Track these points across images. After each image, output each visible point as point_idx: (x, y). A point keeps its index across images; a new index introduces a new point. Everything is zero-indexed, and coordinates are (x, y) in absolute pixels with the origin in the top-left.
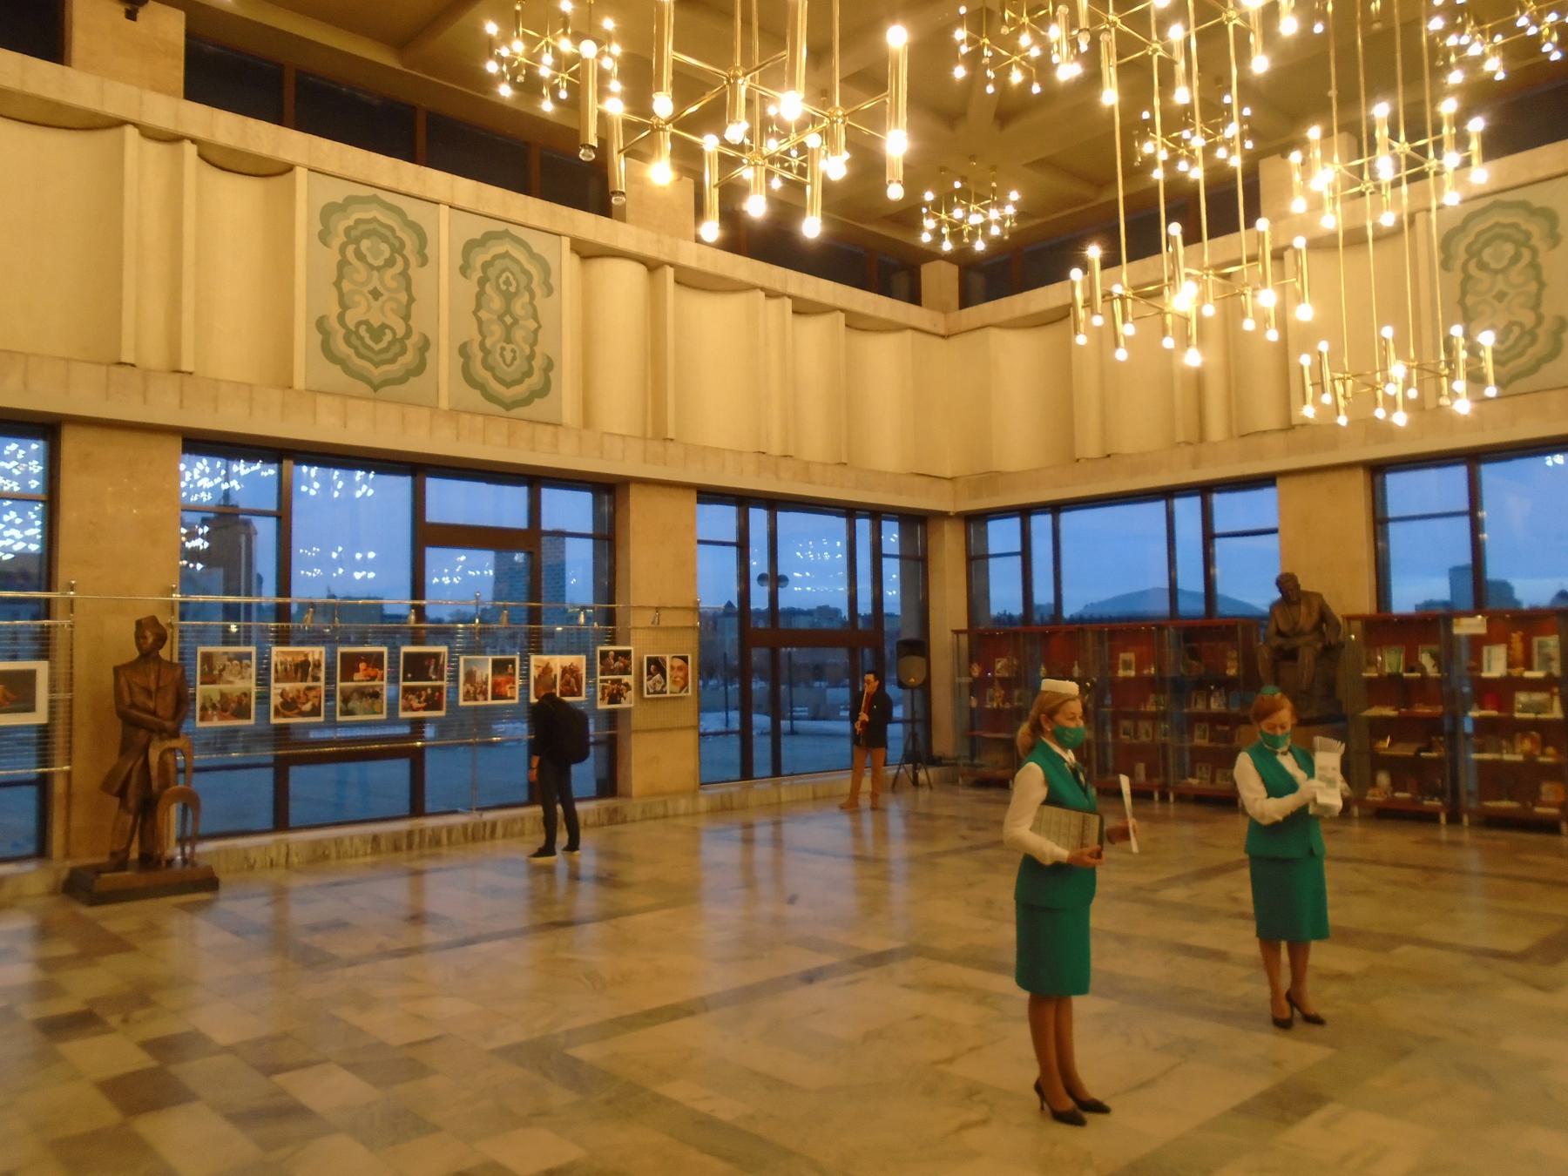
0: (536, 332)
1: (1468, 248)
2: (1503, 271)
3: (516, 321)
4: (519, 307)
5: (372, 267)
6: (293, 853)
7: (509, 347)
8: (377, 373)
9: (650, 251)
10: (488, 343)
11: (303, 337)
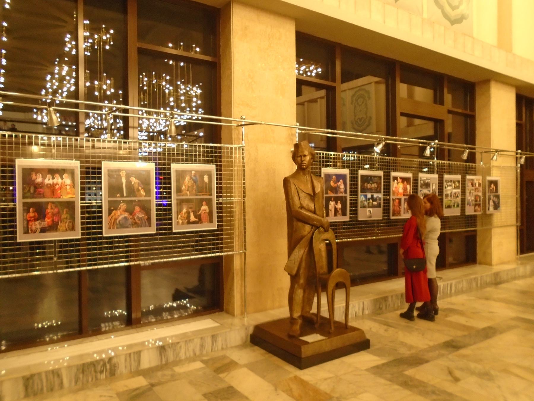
6: (366, 307)
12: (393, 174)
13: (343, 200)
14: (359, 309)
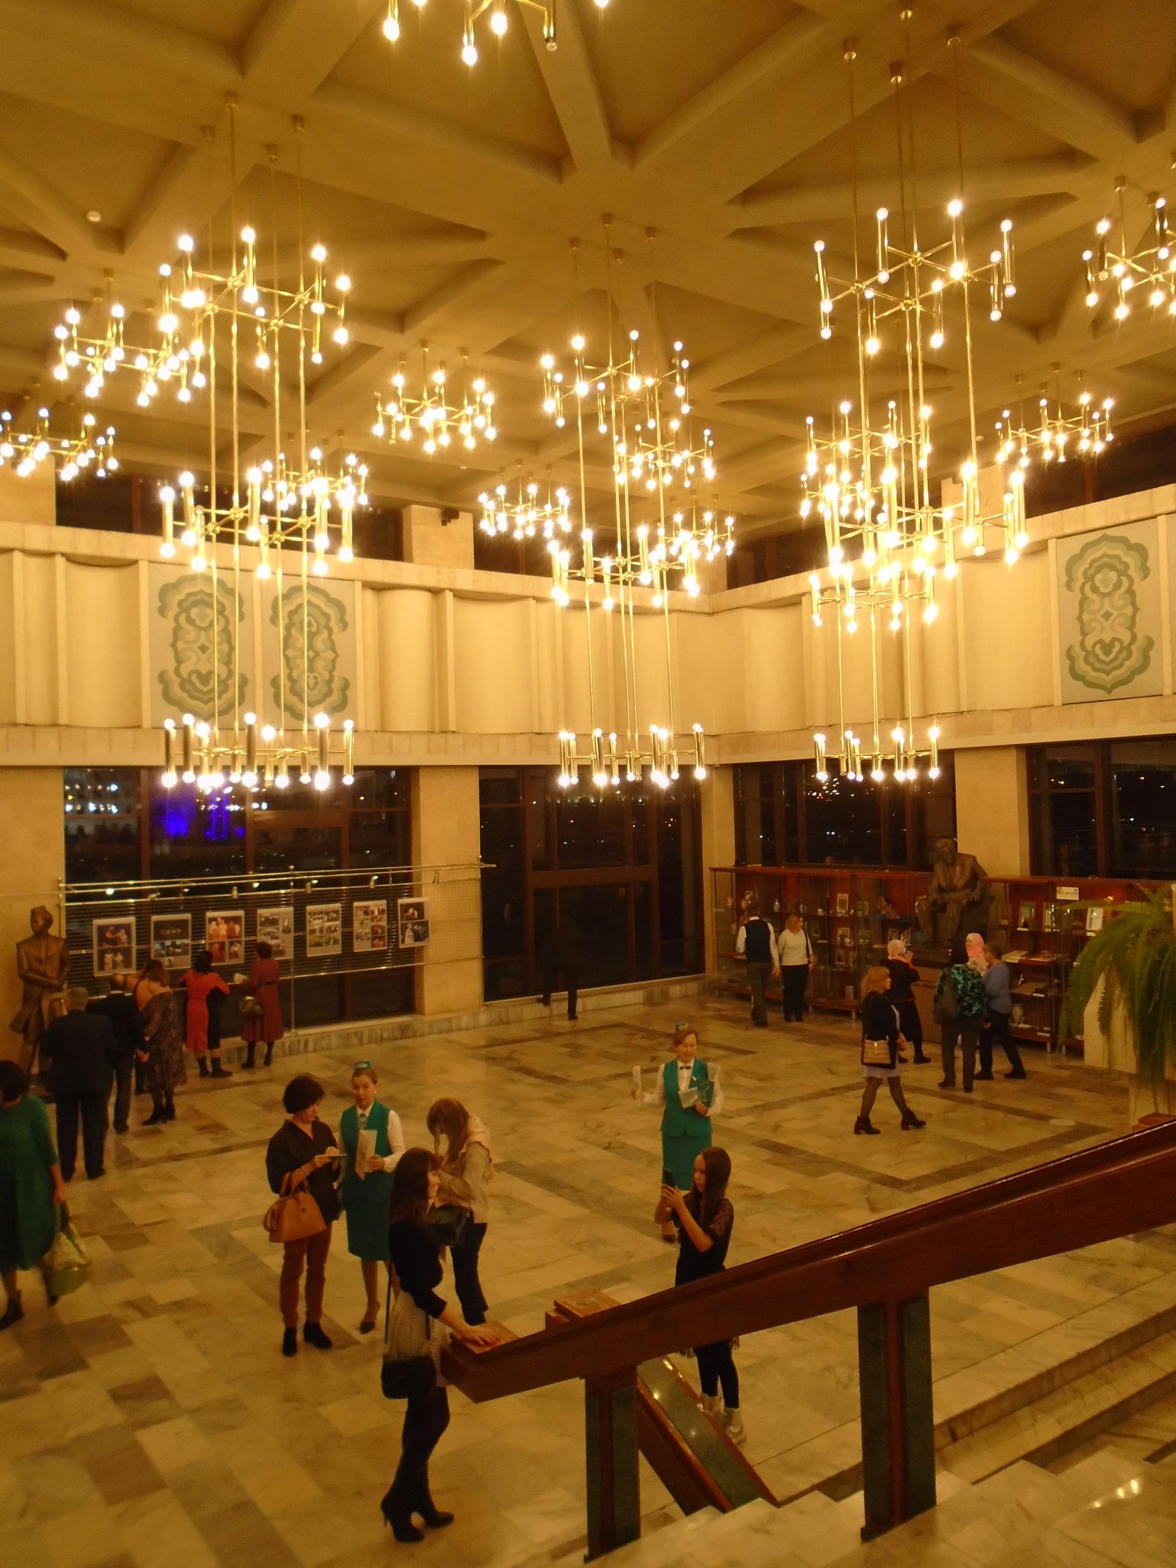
0: (334, 661)
1: (1085, 574)
2: (1109, 594)
3: (317, 654)
4: (319, 643)
5: (200, 629)
7: (312, 675)
9: (432, 583)
10: (295, 675)
11: (148, 687)
12: (210, 914)
13: (127, 952)
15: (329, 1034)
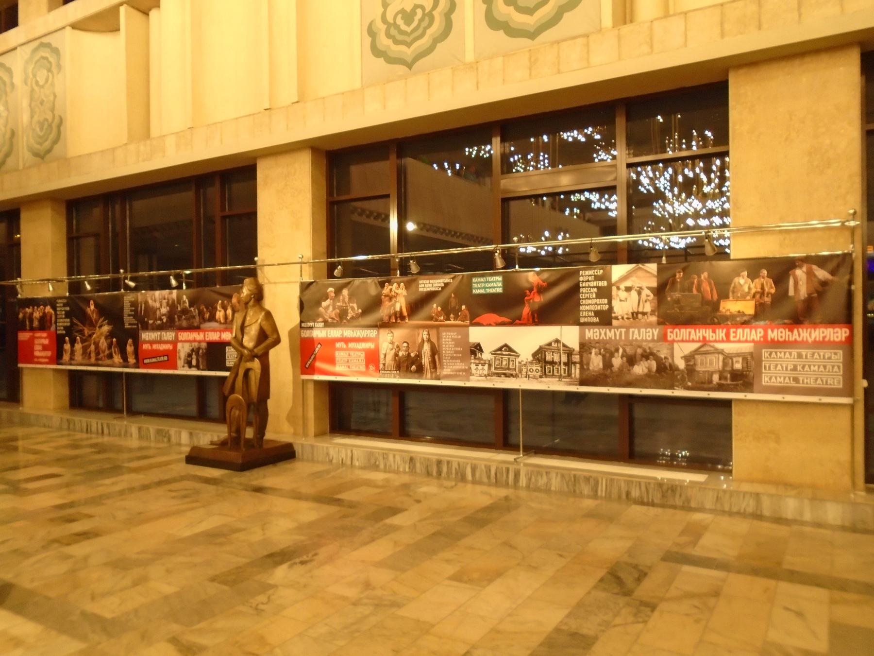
6: (355, 457)
8: (408, 52)
14: (346, 456)
15: (548, 470)
